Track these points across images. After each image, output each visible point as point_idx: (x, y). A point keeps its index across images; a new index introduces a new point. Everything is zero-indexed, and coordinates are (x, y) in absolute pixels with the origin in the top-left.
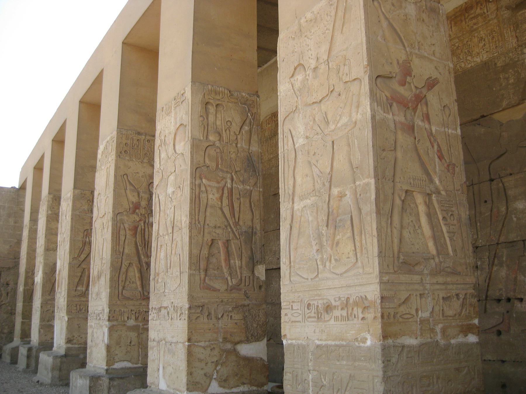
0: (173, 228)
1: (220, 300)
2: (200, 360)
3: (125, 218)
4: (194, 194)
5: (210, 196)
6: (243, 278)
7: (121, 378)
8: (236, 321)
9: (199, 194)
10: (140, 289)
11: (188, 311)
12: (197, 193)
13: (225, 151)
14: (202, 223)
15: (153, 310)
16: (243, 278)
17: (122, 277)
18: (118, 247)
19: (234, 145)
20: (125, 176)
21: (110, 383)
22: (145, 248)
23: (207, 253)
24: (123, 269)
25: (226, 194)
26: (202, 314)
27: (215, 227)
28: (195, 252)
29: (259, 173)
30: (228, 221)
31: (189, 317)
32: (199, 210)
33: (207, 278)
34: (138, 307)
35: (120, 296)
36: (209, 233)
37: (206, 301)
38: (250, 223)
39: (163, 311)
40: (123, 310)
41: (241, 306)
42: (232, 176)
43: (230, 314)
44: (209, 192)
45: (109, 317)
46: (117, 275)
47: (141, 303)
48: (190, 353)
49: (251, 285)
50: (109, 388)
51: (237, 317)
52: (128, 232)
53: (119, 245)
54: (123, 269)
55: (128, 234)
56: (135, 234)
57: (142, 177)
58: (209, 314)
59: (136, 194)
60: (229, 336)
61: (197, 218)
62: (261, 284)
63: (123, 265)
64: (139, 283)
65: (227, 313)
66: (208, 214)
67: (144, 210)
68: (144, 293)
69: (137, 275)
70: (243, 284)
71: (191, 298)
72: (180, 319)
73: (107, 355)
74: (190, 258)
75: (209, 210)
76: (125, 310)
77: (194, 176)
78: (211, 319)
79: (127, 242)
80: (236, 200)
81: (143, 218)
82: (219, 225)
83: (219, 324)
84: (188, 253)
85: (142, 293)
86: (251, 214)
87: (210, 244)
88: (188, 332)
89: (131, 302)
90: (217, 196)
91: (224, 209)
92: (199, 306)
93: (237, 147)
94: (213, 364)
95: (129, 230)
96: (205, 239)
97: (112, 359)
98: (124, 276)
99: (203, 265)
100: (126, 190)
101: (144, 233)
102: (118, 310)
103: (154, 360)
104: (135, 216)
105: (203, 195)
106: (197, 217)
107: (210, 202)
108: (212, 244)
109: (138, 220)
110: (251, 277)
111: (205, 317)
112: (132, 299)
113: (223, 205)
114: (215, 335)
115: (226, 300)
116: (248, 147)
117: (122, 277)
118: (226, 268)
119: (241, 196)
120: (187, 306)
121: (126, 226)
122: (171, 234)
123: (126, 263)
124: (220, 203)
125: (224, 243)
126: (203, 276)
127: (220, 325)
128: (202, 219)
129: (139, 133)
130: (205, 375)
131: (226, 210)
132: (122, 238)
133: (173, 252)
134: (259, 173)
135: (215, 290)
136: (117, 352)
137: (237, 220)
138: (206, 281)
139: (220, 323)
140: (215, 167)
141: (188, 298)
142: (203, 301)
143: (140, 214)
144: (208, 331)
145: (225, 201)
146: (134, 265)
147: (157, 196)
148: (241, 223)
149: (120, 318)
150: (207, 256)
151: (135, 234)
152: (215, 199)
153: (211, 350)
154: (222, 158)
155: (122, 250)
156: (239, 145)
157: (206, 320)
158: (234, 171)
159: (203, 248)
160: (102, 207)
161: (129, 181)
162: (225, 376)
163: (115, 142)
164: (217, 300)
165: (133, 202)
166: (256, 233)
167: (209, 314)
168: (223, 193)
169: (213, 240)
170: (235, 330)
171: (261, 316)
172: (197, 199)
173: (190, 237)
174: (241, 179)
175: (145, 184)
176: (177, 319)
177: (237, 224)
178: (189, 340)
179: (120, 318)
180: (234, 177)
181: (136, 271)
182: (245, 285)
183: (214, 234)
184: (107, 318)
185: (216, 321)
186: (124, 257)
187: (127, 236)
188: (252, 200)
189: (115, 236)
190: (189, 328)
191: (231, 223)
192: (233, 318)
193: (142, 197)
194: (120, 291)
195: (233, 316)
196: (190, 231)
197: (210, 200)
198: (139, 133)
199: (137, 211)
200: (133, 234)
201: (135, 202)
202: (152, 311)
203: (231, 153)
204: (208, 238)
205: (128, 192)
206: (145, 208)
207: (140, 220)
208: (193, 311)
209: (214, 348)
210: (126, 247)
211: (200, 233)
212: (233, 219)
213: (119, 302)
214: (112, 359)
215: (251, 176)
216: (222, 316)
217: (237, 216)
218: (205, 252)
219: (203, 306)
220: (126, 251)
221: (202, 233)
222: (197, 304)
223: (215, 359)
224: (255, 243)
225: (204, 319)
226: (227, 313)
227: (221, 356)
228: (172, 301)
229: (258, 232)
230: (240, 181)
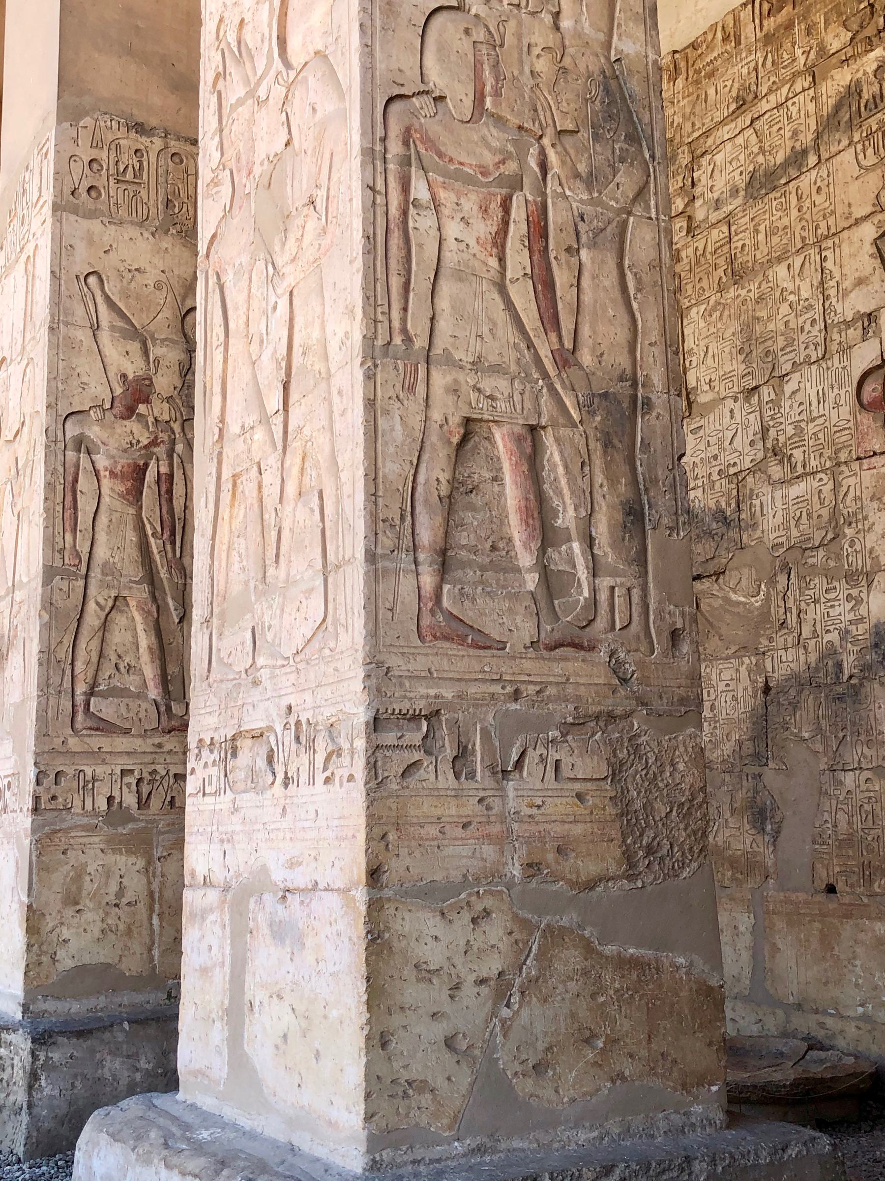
0: (286, 386)
1: (509, 689)
2: (425, 973)
3: (94, 432)
4: (380, 211)
5: (453, 229)
6: (603, 596)
7: (81, 1034)
8: (578, 786)
9: (405, 213)
10: (154, 692)
11: (369, 740)
12: (394, 211)
13: (509, 40)
14: (420, 343)
15: (205, 753)
16: (603, 596)
17: (88, 647)
18: (68, 537)
19: (547, 19)
20: (92, 280)
21: (33, 1053)
22: (173, 543)
23: (444, 477)
24: (93, 617)
25: (518, 229)
26: (428, 753)
27: (477, 364)
28: (393, 469)
29: (651, 149)
30: (530, 346)
31: (372, 766)
32: (406, 287)
33: (446, 588)
34: (148, 759)
35: (80, 717)
36: (454, 390)
37: (448, 693)
38: (623, 360)
39: (249, 755)
40: (89, 771)
41: (597, 718)
42: (543, 152)
43: (554, 755)
44: (446, 212)
45: (37, 799)
46: (68, 640)
47: (160, 746)
48: (378, 942)
49: (635, 627)
50: (33, 1077)
51: (583, 763)
52: (106, 483)
53: (74, 530)
54: (93, 617)
55: (105, 491)
56: (135, 494)
57: (158, 286)
58: (462, 755)
59: (135, 347)
60: (550, 857)
61: (396, 324)
62: (679, 625)
63: (91, 606)
64: (150, 671)
65: (541, 750)
66: (443, 303)
67: (166, 405)
68: (169, 709)
69: (145, 641)
70: (601, 623)
71: (379, 673)
72: (327, 781)
73: (29, 946)
74: (373, 496)
75: (446, 287)
76: (100, 770)
77: (380, 133)
78: (471, 776)
79: (103, 519)
80: (563, 256)
81: (164, 436)
82: (493, 359)
83: (504, 797)
84: (361, 472)
85: (163, 709)
86: (624, 318)
87: (455, 440)
88: (369, 839)
89: (122, 743)
90: (484, 228)
91: (514, 292)
92: (415, 718)
93: (558, 28)
94: (485, 990)
95: (113, 474)
96: (436, 415)
97: (45, 959)
98: (95, 645)
99: (428, 531)
100: (95, 328)
101: (170, 491)
102: (70, 771)
103: (205, 971)
104: (132, 425)
105: (422, 223)
106: (396, 315)
107: (450, 257)
108: (465, 439)
109: (146, 442)
110: (636, 593)
111: (446, 767)
112: (127, 732)
113: (509, 275)
114: (489, 851)
115: (532, 689)
116: (602, 37)
117: (88, 647)
118: (526, 546)
119: (584, 239)
120: (361, 715)
121: (102, 462)
122: (280, 418)
123: (98, 595)
124: (493, 262)
125: (519, 439)
126: (428, 580)
127: (512, 804)
128: (418, 327)
129: (140, 128)
130: (449, 1043)
131: (523, 297)
132: (86, 506)
133: (291, 489)
134: (651, 149)
135: (484, 643)
136: (66, 933)
137: (568, 344)
138: (446, 603)
139: (511, 794)
140: (468, 103)
141: (368, 676)
142: (432, 692)
143: (151, 420)
144: (459, 832)
145: (518, 259)
146: (132, 603)
147: (212, 280)
148: (586, 358)
149: (77, 803)
150: (444, 490)
151: (135, 494)
152: (472, 243)
153: (474, 921)
154: (496, 66)
155: (84, 550)
156: (566, 23)
157: (447, 779)
158: (550, 131)
159: (425, 457)
160: (11, 404)
161: (107, 299)
162: (541, 1046)
163: (51, 155)
164: (497, 688)
165: (124, 376)
166: (648, 404)
167: (462, 755)
168: (505, 223)
169: (468, 421)
170: (578, 830)
171: (681, 766)
172: (396, 240)
173: (370, 404)
174: (582, 168)
175: (167, 313)
176: (312, 781)
177: (566, 359)
178: (374, 874)
179: (77, 803)
180: (553, 157)
181: (140, 627)
182: (613, 628)
183: (473, 396)
184: (29, 803)
185: (489, 783)
186: (96, 574)
187: (106, 499)
188: (627, 263)
189: (59, 499)
190: (372, 820)
191: (544, 352)
192: (566, 772)
193: (157, 360)
194: (80, 699)
195: (567, 761)
196: (370, 377)
197: (450, 243)
198: (140, 128)
199: (142, 408)
200: (128, 492)
201: (131, 376)
202: (198, 756)
203: (536, 51)
204: (447, 411)
205: (105, 337)
206: (169, 399)
207: (154, 443)
208: (389, 738)
209: (487, 913)
210: (102, 537)
211: (412, 389)
212: (553, 336)
213: (73, 743)
214: (45, 959)
215: (622, 160)
216: (519, 764)
217: (567, 324)
218: (436, 472)
219: (433, 716)
220: (102, 553)
221: (421, 388)
222: (405, 706)
223: (492, 966)
224: (646, 446)
225: (437, 776)
226: (541, 750)
227: (521, 949)
228: (285, 702)
229: (653, 397)
230: (577, 175)
